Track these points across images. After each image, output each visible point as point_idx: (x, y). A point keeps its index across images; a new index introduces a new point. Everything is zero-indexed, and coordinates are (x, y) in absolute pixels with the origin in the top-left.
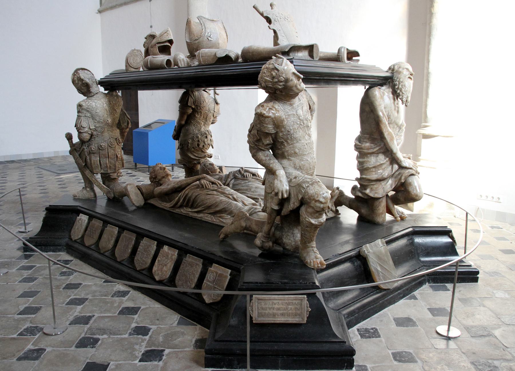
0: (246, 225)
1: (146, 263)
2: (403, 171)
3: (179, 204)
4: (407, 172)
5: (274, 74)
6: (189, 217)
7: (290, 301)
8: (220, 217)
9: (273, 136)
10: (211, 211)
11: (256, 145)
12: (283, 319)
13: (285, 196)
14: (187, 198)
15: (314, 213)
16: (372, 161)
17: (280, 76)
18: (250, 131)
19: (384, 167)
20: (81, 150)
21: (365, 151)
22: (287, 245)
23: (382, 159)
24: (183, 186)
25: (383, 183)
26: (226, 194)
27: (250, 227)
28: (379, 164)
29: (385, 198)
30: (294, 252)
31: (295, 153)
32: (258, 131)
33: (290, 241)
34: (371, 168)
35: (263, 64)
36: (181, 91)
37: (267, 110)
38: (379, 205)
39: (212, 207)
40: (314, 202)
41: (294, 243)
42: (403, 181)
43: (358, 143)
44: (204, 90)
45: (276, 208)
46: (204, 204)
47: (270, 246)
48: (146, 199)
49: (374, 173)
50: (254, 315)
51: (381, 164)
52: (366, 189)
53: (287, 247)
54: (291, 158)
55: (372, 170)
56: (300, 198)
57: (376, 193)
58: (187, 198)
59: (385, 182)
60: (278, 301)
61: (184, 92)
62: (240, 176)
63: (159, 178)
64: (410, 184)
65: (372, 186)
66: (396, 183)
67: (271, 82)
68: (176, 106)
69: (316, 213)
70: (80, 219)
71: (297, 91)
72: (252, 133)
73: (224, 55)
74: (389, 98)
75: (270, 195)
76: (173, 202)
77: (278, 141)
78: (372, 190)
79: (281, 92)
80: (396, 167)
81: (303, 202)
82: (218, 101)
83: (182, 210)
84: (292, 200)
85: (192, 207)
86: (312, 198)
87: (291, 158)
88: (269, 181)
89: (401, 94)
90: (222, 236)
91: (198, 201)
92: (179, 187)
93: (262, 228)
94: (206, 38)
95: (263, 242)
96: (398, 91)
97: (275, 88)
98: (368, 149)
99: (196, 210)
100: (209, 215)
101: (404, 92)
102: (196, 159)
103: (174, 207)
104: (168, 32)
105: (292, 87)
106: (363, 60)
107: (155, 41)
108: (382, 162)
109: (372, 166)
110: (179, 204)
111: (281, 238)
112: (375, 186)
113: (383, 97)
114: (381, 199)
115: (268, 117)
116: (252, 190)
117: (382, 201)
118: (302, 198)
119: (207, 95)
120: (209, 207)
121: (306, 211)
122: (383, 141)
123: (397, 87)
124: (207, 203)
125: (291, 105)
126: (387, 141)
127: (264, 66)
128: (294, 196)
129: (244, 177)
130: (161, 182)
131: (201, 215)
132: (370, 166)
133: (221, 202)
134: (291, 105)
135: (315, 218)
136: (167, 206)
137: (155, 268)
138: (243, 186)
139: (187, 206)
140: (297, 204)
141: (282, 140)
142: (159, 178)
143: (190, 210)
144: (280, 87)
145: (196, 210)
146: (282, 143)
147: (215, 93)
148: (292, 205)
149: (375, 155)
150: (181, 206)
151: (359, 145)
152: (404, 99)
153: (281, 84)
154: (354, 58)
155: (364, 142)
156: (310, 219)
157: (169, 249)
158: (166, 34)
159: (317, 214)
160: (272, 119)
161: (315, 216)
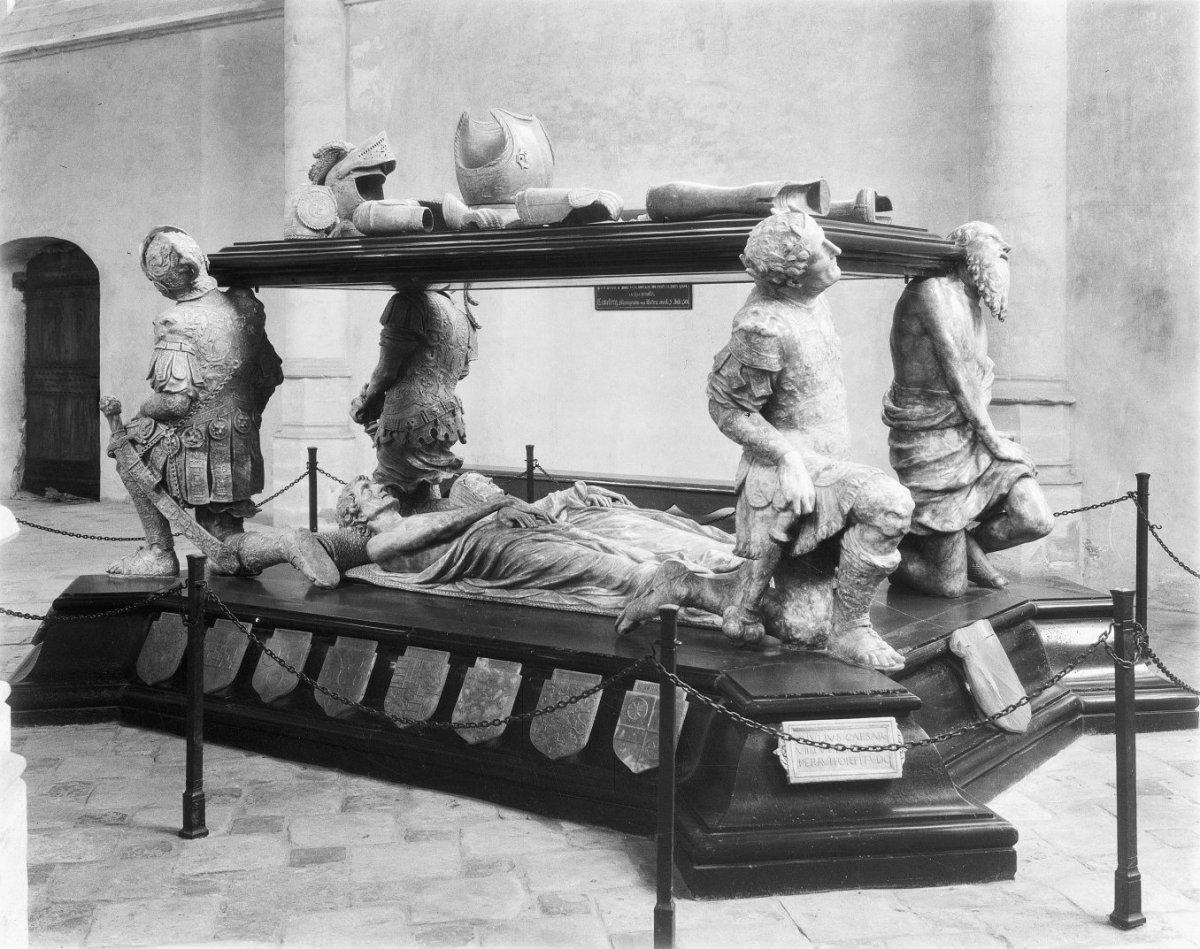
0: (689, 593)
1: (425, 709)
2: (1002, 468)
3: (454, 570)
4: (1013, 471)
5: (790, 245)
6: (483, 602)
7: (862, 731)
8: (576, 593)
9: (774, 377)
10: (554, 579)
11: (734, 400)
12: (852, 772)
13: (809, 508)
14: (478, 554)
15: (881, 542)
16: (930, 447)
17: (801, 249)
18: (717, 372)
19: (958, 459)
21: (915, 424)
22: (798, 631)
23: (953, 441)
24: (459, 526)
25: (959, 497)
28: (947, 453)
29: (963, 534)
30: (813, 645)
31: (817, 416)
32: (743, 366)
33: (803, 620)
35: (755, 223)
36: (379, 297)
37: (768, 321)
38: (953, 549)
39: (555, 570)
40: (882, 515)
41: (813, 624)
42: (1005, 491)
43: (891, 405)
44: (441, 292)
47: (761, 634)
50: (790, 762)
51: (954, 453)
53: (798, 636)
54: (808, 428)
55: (932, 467)
57: (945, 521)
58: (478, 554)
59: (963, 496)
60: (837, 732)
61: (395, 298)
62: (579, 503)
63: (367, 512)
64: (1022, 497)
65: (934, 506)
66: (989, 496)
67: (782, 261)
68: (373, 334)
71: (827, 281)
73: (590, 203)
74: (961, 301)
75: (759, 513)
76: (432, 570)
77: (784, 390)
79: (796, 282)
80: (985, 460)
81: (851, 519)
82: (478, 320)
83: (461, 587)
85: (489, 577)
87: (808, 428)
89: (988, 291)
94: (514, 162)
95: (745, 623)
96: (982, 287)
97: (786, 275)
98: (921, 419)
99: (503, 583)
100: (547, 593)
101: (995, 289)
102: (426, 472)
104: (384, 143)
105: (820, 272)
107: (344, 165)
109: (932, 459)
110: (454, 570)
111: (779, 615)
112: (943, 505)
113: (945, 297)
114: (956, 536)
117: (958, 541)
118: (852, 511)
119: (448, 303)
120: (543, 572)
122: (955, 399)
123: (976, 278)
125: (809, 310)
126: (965, 400)
127: (756, 231)
129: (593, 503)
130: (372, 524)
131: (519, 594)
132: (928, 460)
133: (577, 556)
134: (809, 310)
136: (409, 581)
139: (475, 575)
140: (837, 526)
141: (793, 387)
142: (367, 512)
143: (488, 584)
144: (798, 272)
145: (503, 583)
146: (791, 394)
147: (468, 299)
149: (938, 432)
151: (898, 412)
152: (997, 305)
153: (802, 265)
155: (907, 403)
156: (871, 556)
157: (492, 666)
158: (378, 148)
159: (886, 545)
160: (779, 340)
161: (881, 549)
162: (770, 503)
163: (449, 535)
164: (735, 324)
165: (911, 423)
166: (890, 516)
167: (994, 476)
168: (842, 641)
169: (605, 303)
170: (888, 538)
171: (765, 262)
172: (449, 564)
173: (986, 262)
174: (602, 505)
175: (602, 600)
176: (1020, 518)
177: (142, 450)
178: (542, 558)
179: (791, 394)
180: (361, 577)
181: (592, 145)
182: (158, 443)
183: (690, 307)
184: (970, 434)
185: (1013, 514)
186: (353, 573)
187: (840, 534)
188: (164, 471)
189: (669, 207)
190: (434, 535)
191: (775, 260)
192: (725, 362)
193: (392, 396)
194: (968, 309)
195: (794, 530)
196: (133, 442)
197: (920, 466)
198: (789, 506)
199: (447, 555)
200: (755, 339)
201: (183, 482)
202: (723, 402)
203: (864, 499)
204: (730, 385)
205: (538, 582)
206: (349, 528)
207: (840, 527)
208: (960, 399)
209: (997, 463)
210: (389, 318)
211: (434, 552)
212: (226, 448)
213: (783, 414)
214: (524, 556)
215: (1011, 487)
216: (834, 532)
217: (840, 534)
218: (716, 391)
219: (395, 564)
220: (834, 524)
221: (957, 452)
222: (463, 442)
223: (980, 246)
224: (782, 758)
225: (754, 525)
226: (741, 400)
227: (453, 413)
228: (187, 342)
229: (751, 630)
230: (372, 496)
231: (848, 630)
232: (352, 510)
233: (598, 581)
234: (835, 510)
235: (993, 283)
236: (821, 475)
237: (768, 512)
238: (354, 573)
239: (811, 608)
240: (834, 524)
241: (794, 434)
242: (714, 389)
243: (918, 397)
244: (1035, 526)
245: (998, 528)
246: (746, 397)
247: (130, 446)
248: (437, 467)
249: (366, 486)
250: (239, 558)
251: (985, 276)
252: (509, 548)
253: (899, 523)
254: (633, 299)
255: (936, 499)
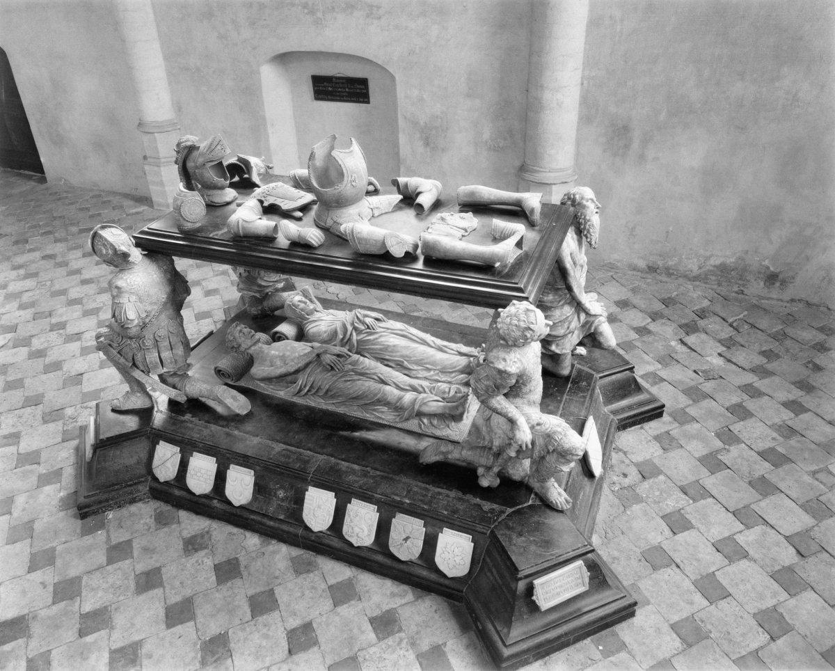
26: (367, 374)
28: (565, 317)
49: (560, 328)
57: (563, 349)
74: (573, 239)
78: (557, 345)
80: (583, 316)
98: (551, 302)
116: (390, 350)
138: (374, 344)
158: (219, 147)
165: (547, 304)
169: (320, 97)
173: (588, 218)
174: (374, 329)
181: (306, 11)
183: (368, 102)
189: (435, 255)
194: (576, 242)
208: (573, 294)
212: (167, 343)
223: (584, 207)
224: (537, 601)
228: (132, 295)
235: (591, 230)
241: (518, 401)
248: (273, 281)
251: (587, 227)
254: (334, 96)
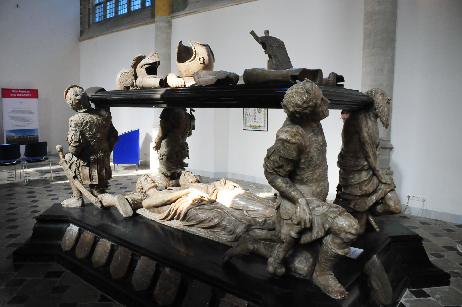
0: (254, 249)
2: (383, 186)
11: (276, 171)
13: (308, 225)
18: (268, 157)
19: (366, 183)
20: (71, 162)
22: (300, 270)
24: (173, 200)
27: (258, 250)
28: (362, 180)
33: (303, 266)
34: (356, 184)
40: (344, 233)
45: (294, 234)
46: (197, 219)
48: (134, 209)
52: (350, 204)
53: (300, 272)
56: (326, 229)
65: (356, 201)
67: (301, 107)
69: (344, 244)
70: (71, 230)
72: (272, 159)
75: (285, 221)
77: (300, 168)
84: (315, 230)
86: (342, 229)
87: (310, 184)
88: (286, 207)
90: (226, 258)
91: (190, 215)
92: (169, 201)
93: (271, 252)
95: (276, 268)
100: (202, 230)
103: (163, 219)
106: (347, 85)
108: (365, 179)
110: (170, 217)
112: (359, 201)
115: (294, 143)
118: (329, 229)
120: (201, 222)
121: (333, 241)
124: (200, 218)
128: (318, 225)
130: (147, 193)
132: (355, 183)
135: (342, 249)
137: (156, 291)
139: (178, 219)
140: (321, 234)
142: (145, 189)
147: (191, 110)
148: (315, 235)
150: (172, 219)
154: (338, 83)
159: (345, 245)
162: (290, 218)
163: (169, 202)
164: (278, 136)
166: (348, 234)
167: (380, 189)
168: (320, 279)
170: (345, 243)
171: (292, 107)
172: (169, 214)
175: (222, 237)
176: (389, 206)
177: (69, 164)
178: (203, 216)
179: (303, 169)
180: (140, 213)
182: (73, 163)
184: (371, 173)
185: (386, 204)
186: (138, 211)
187: (323, 238)
188: (75, 172)
190: (164, 202)
191: (297, 106)
192: (272, 153)
193: (164, 142)
195: (301, 233)
196: (66, 161)
197: (351, 185)
198: (299, 224)
199: (168, 210)
200: (287, 145)
201: (82, 176)
202: (271, 172)
203: (336, 224)
204: (274, 165)
205: (199, 225)
206: (140, 194)
207: (323, 235)
209: (381, 184)
210: (162, 116)
211: (165, 208)
213: (298, 178)
214: (195, 215)
215: (386, 194)
216: (320, 237)
217: (323, 238)
218: (268, 166)
219: (152, 210)
220: (320, 233)
221: (365, 181)
222: (189, 158)
225: (283, 226)
226: (279, 172)
227: (184, 149)
229: (279, 270)
230: (147, 183)
231: (323, 275)
232: (140, 187)
233: (222, 228)
234: (321, 227)
236: (316, 209)
237: (289, 221)
238: (138, 211)
239: (306, 261)
240: (320, 233)
242: (266, 165)
243: (352, 157)
244: (395, 210)
245: (379, 208)
246: (281, 170)
247: (65, 163)
249: (146, 179)
250: (101, 202)
252: (190, 211)
253: (352, 237)
255: (357, 198)
